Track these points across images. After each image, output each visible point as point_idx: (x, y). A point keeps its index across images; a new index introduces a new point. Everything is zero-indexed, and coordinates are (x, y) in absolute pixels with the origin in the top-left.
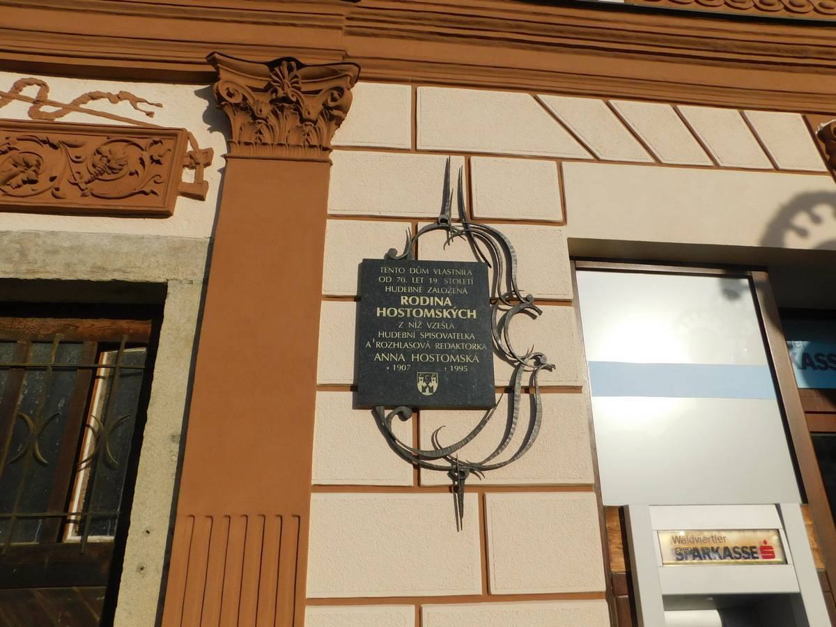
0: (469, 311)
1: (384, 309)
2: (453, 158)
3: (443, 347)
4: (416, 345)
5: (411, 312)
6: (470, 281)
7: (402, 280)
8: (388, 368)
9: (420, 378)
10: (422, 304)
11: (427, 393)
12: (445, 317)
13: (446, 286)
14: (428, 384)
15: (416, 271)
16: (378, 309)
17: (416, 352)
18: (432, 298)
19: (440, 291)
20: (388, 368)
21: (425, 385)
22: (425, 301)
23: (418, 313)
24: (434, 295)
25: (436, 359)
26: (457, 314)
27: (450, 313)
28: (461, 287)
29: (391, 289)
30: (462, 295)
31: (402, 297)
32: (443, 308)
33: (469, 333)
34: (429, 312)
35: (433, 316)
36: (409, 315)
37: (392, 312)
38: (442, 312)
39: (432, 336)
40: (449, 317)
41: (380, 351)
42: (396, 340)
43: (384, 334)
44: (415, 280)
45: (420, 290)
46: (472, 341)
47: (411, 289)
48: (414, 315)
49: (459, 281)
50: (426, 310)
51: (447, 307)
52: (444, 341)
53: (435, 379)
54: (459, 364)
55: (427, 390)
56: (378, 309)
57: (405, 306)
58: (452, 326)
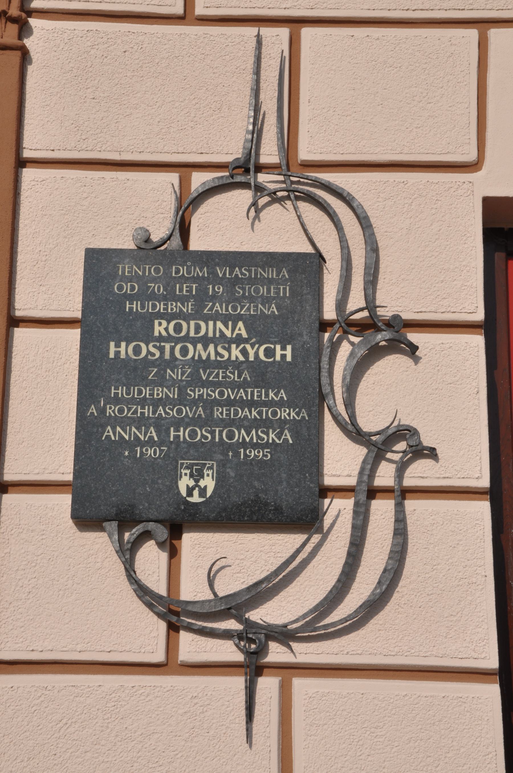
0: (278, 347)
1: (123, 344)
2: (266, 32)
3: (229, 415)
4: (179, 411)
5: (172, 349)
6: (285, 289)
7: (158, 288)
8: (127, 453)
9: (184, 472)
10: (192, 334)
11: (196, 498)
12: (233, 358)
13: (238, 300)
14: (197, 481)
15: (183, 271)
16: (112, 344)
17: (178, 424)
18: (211, 323)
19: (227, 310)
20: (127, 453)
21: (192, 483)
22: (198, 328)
23: (184, 351)
24: (215, 317)
25: (213, 437)
26: (257, 354)
27: (244, 352)
28: (266, 301)
29: (136, 306)
30: (267, 316)
31: (156, 322)
32: (231, 341)
33: (277, 388)
34: (205, 349)
35: (213, 357)
36: (167, 356)
37: (137, 350)
38: (229, 350)
39: (208, 394)
40: (241, 358)
41: (115, 421)
42: (143, 402)
43: (121, 391)
44: (181, 290)
45: (188, 308)
46: (281, 404)
47: (173, 307)
48: (177, 354)
49: (263, 290)
50: (199, 346)
51: (239, 340)
52: (229, 403)
53: (210, 472)
54: (255, 446)
55: (196, 492)
56: (112, 344)
57: (161, 339)
58: (246, 375)
